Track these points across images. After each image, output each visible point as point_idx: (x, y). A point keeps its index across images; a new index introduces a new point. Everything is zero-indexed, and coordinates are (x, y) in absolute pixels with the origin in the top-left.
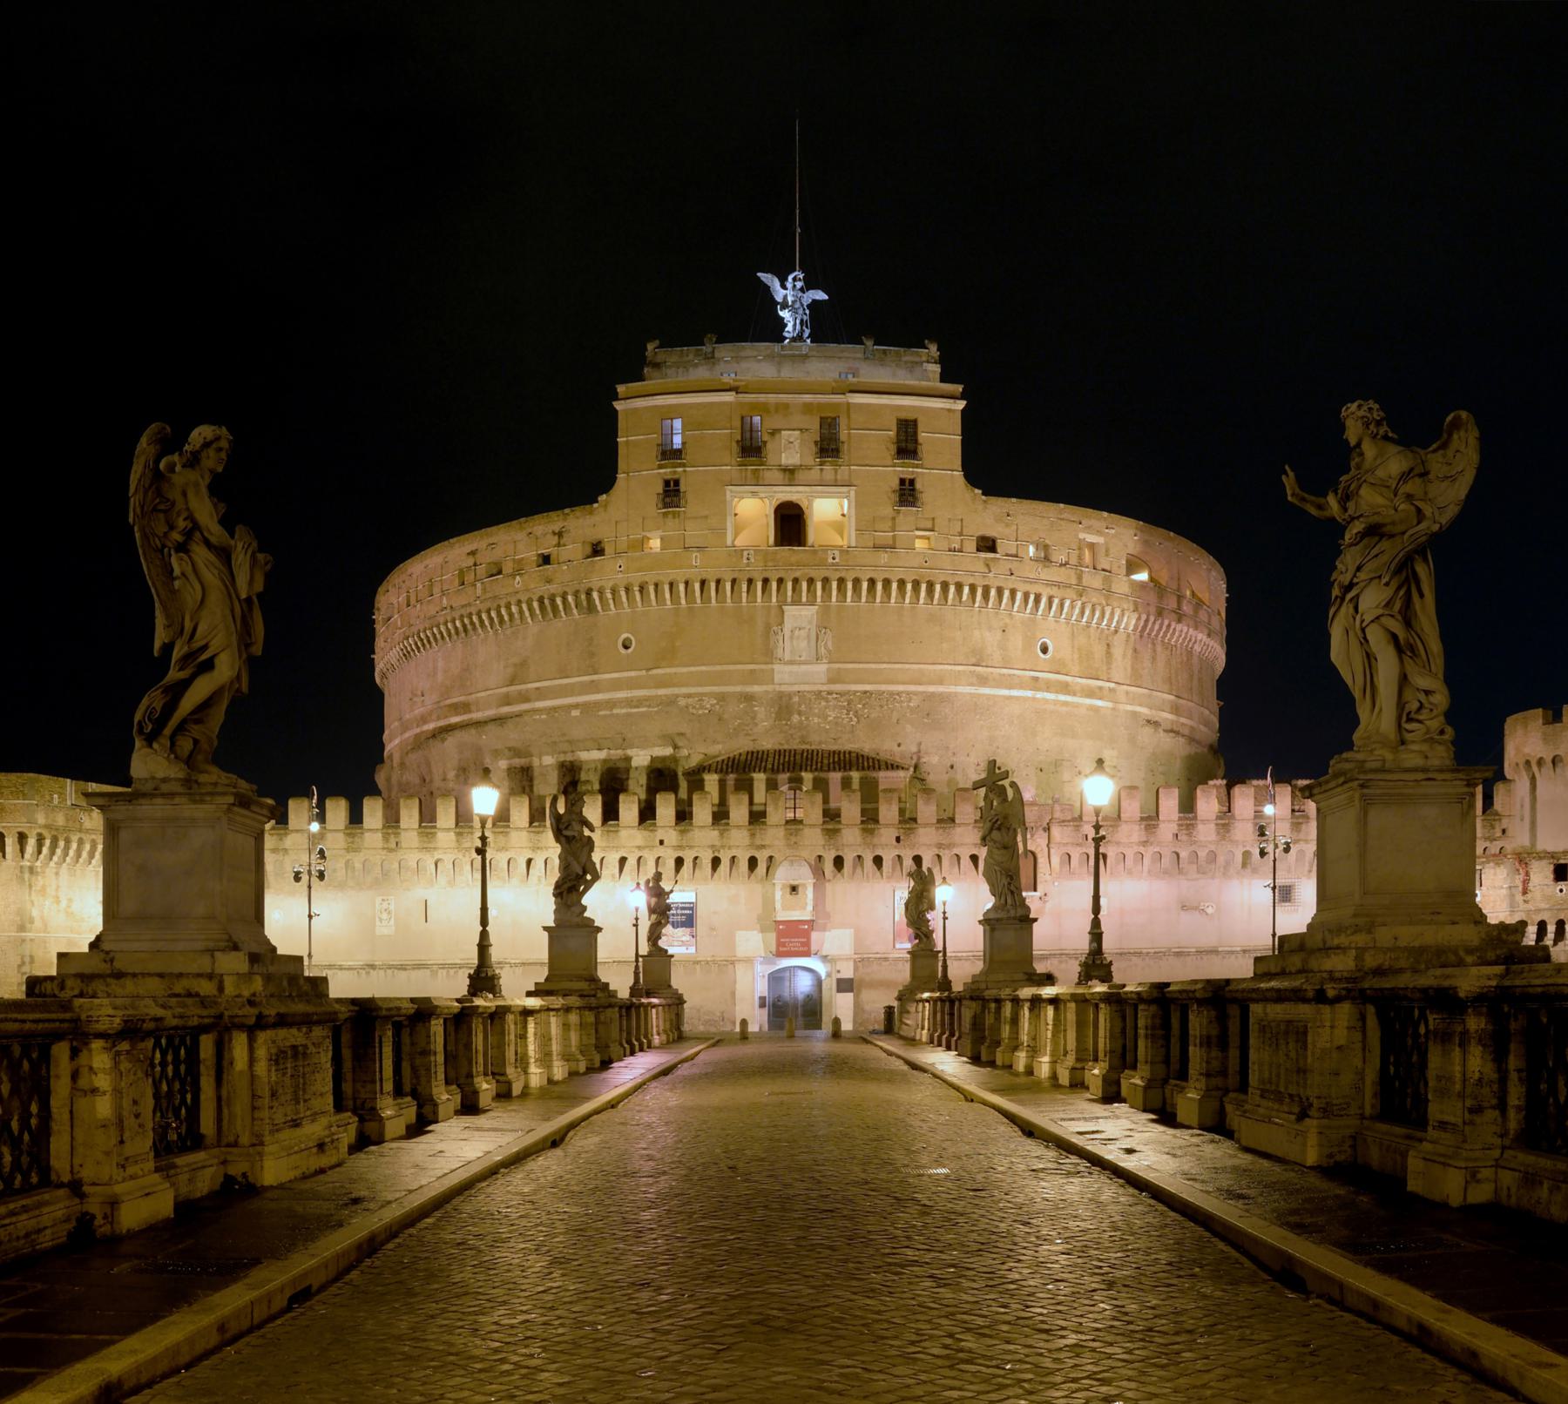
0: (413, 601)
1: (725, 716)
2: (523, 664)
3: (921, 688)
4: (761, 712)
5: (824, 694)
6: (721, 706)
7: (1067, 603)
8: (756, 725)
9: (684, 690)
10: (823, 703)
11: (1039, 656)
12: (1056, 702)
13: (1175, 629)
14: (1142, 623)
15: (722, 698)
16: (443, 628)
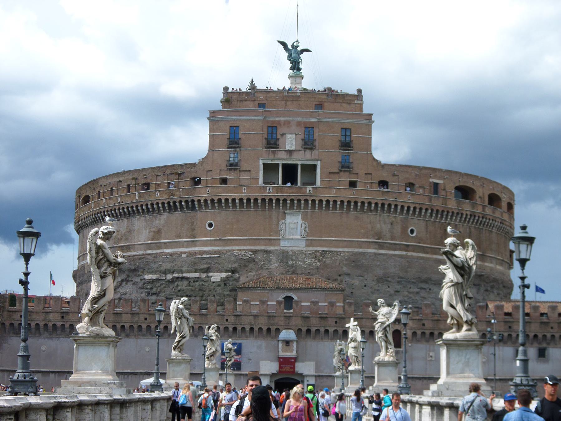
0: (101, 195)
1: (256, 260)
2: (159, 232)
3: (350, 250)
4: (273, 258)
5: (303, 251)
6: (255, 255)
7: (424, 211)
8: (272, 265)
9: (237, 248)
10: (304, 256)
11: (409, 236)
12: (418, 258)
13: (481, 222)
14: (463, 219)
15: (255, 252)
16: (117, 211)
